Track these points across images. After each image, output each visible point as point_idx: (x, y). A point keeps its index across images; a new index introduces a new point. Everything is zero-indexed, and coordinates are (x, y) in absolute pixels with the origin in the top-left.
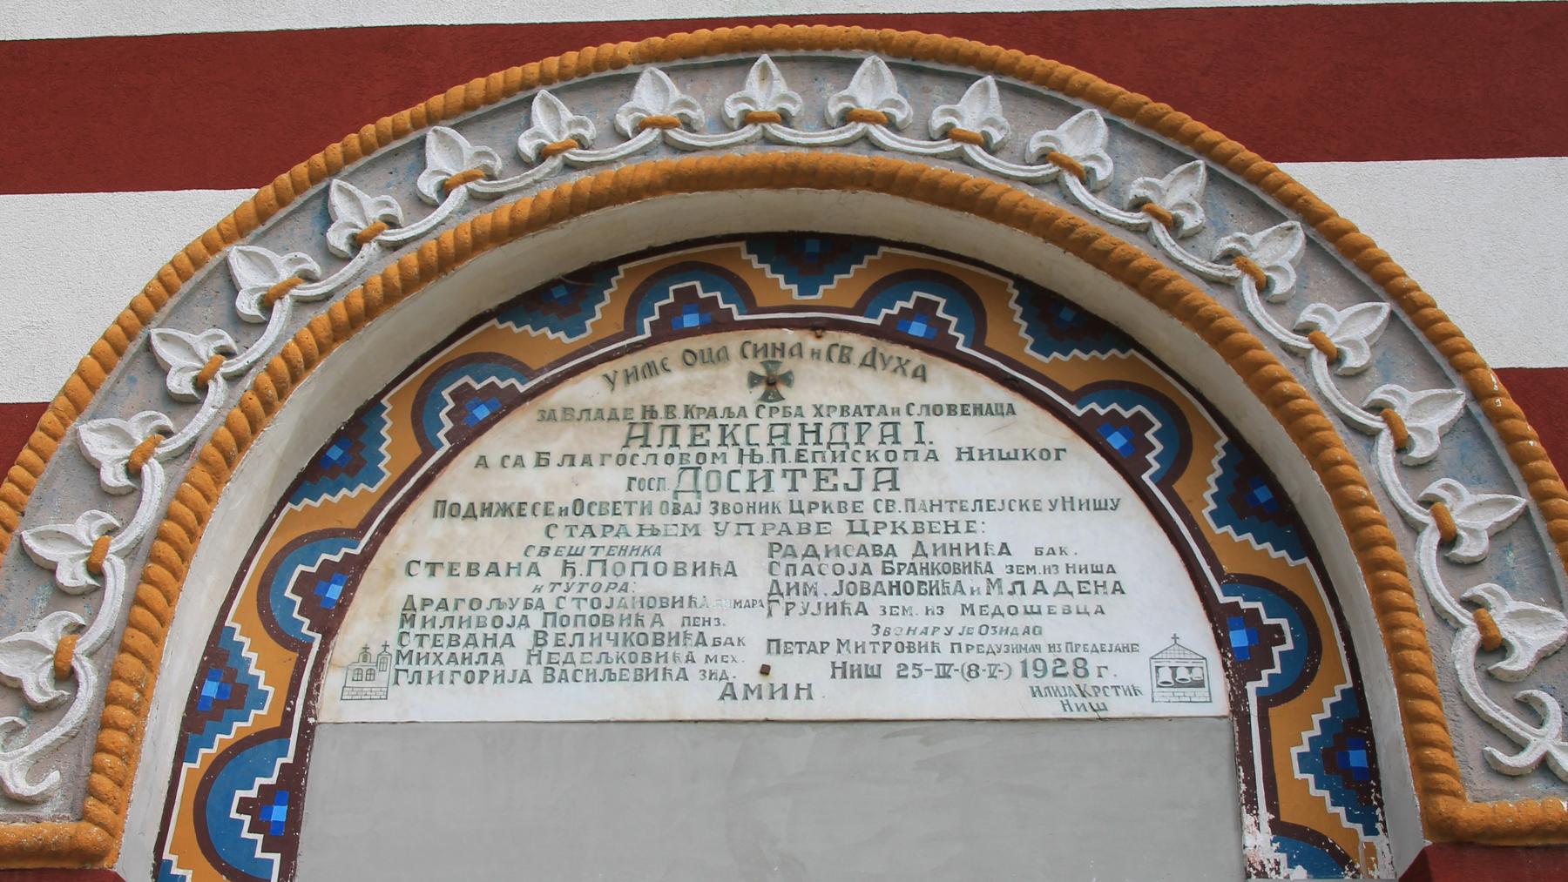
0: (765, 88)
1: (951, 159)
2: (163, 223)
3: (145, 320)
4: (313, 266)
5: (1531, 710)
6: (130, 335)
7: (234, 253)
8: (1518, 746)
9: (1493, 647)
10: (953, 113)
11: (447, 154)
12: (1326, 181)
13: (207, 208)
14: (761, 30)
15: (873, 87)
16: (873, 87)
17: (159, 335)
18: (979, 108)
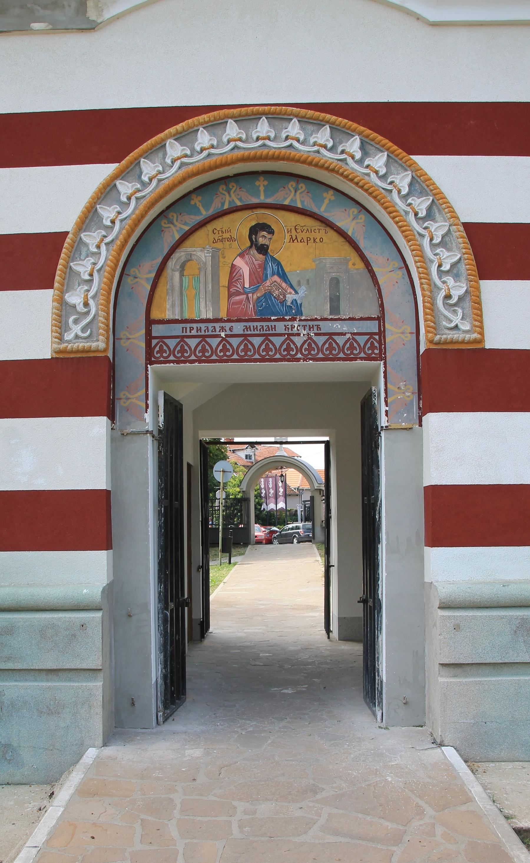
0: (263, 128)
1: (315, 152)
2: (95, 174)
3: (95, 203)
4: (139, 186)
5: (455, 312)
6: (92, 208)
7: (118, 183)
8: (451, 321)
9: (448, 297)
10: (317, 137)
11: (174, 150)
12: (421, 160)
13: (107, 170)
14: (261, 109)
15: (294, 129)
16: (294, 129)
17: (100, 208)
18: (324, 136)
